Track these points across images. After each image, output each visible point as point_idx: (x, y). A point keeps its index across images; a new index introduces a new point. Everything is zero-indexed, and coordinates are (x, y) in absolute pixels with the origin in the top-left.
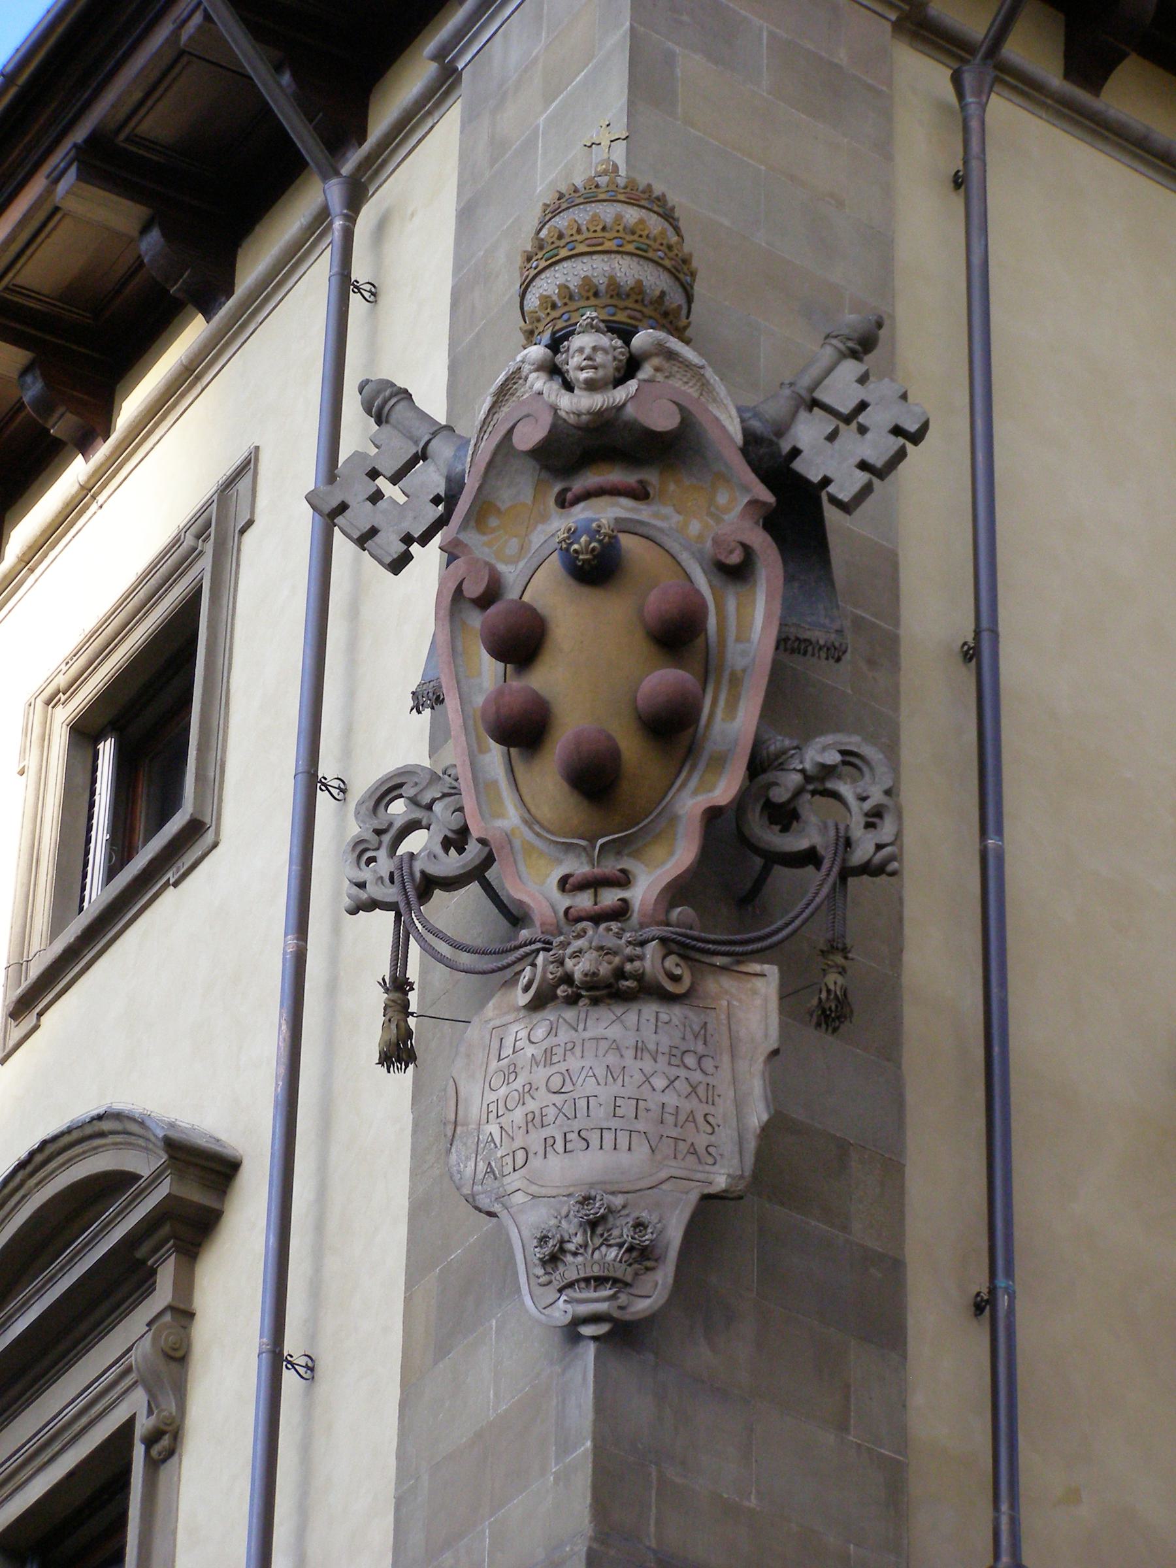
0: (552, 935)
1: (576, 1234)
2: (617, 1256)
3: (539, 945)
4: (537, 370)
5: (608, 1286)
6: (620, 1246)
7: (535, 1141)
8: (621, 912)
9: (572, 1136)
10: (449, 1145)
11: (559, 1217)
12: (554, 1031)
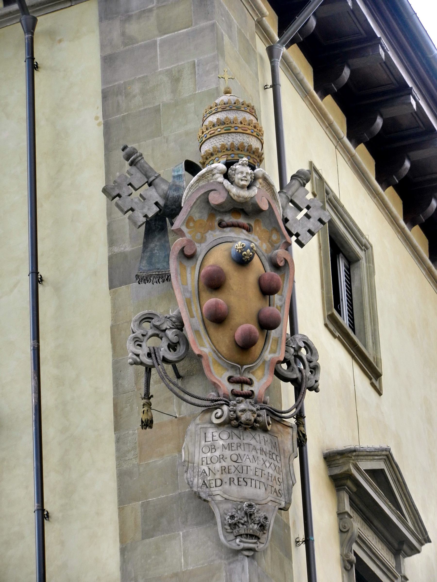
4: (220, 173)
7: (226, 478)
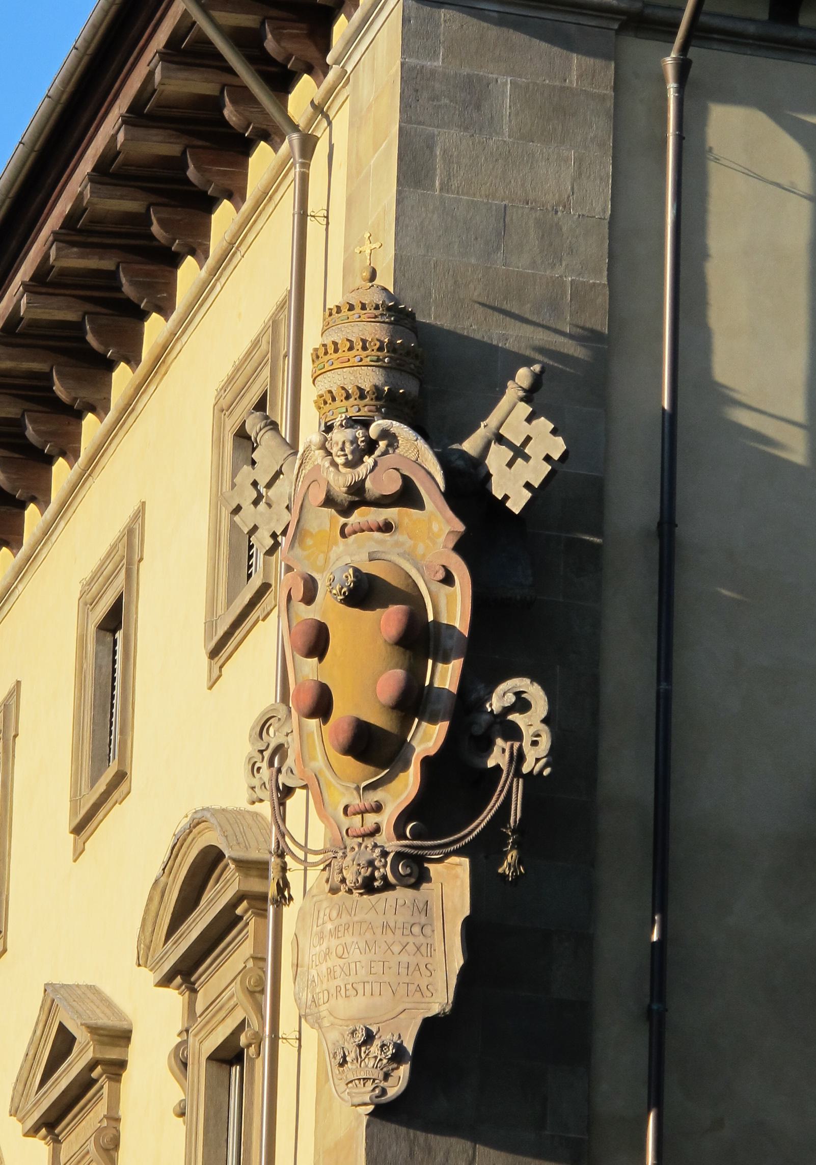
8: (377, 830)
9: (349, 987)
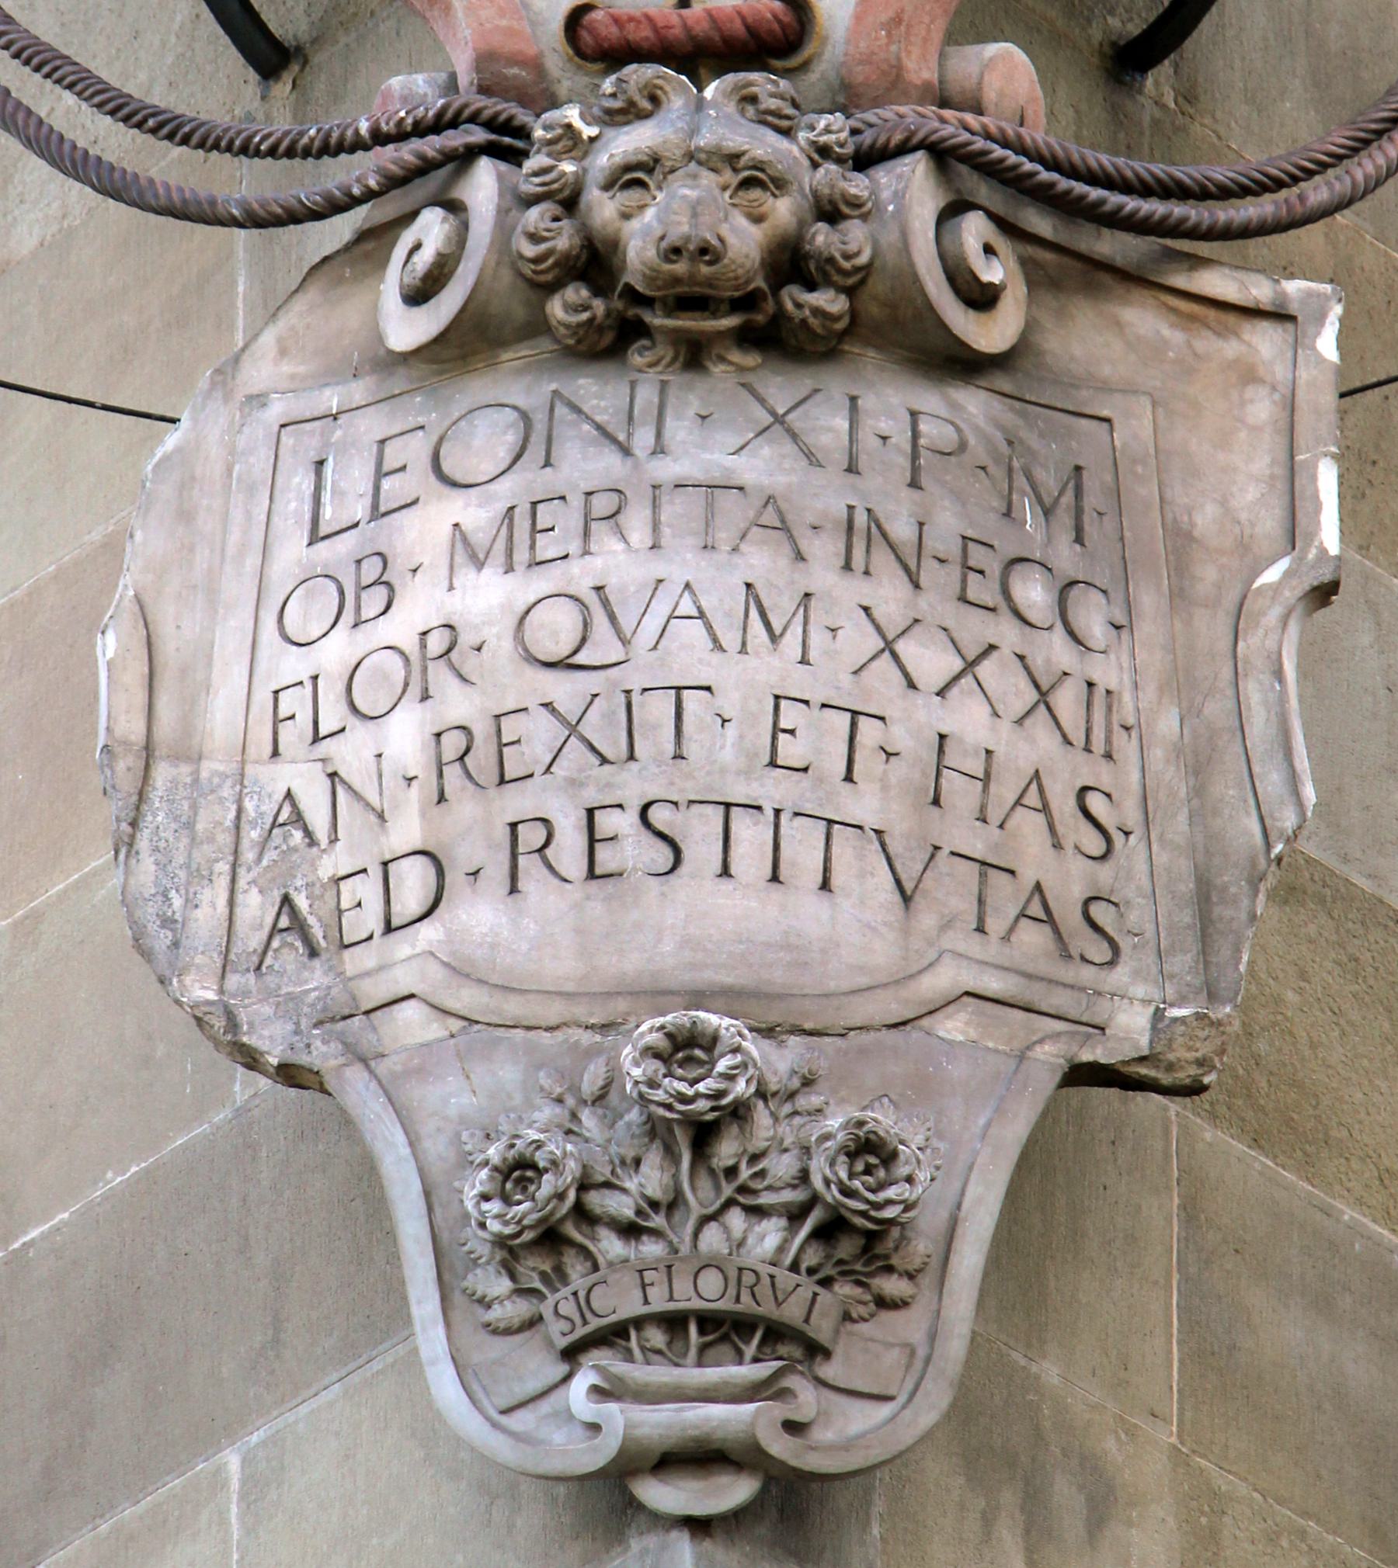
0: (524, 101)
1: (637, 1162)
2: (781, 1249)
3: (478, 135)
5: (750, 1350)
6: (795, 1215)
10: (125, 827)
11: (570, 1101)
12: (536, 450)
